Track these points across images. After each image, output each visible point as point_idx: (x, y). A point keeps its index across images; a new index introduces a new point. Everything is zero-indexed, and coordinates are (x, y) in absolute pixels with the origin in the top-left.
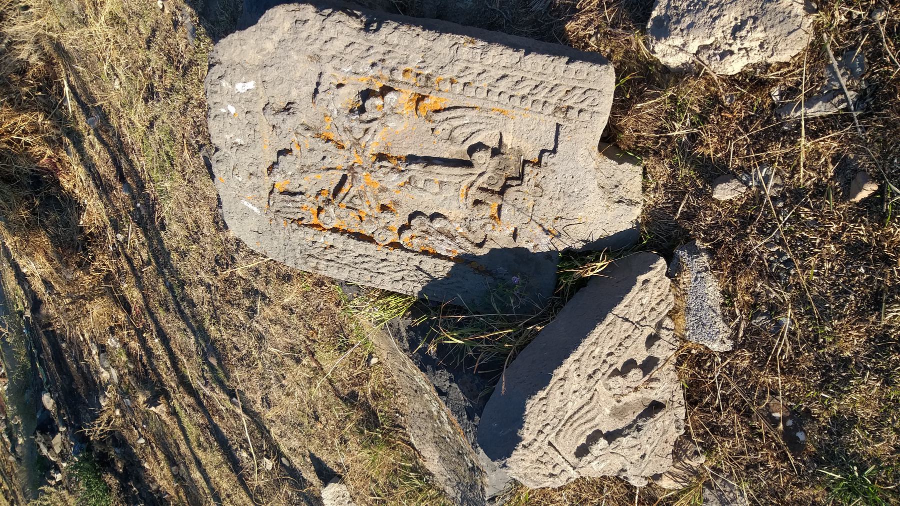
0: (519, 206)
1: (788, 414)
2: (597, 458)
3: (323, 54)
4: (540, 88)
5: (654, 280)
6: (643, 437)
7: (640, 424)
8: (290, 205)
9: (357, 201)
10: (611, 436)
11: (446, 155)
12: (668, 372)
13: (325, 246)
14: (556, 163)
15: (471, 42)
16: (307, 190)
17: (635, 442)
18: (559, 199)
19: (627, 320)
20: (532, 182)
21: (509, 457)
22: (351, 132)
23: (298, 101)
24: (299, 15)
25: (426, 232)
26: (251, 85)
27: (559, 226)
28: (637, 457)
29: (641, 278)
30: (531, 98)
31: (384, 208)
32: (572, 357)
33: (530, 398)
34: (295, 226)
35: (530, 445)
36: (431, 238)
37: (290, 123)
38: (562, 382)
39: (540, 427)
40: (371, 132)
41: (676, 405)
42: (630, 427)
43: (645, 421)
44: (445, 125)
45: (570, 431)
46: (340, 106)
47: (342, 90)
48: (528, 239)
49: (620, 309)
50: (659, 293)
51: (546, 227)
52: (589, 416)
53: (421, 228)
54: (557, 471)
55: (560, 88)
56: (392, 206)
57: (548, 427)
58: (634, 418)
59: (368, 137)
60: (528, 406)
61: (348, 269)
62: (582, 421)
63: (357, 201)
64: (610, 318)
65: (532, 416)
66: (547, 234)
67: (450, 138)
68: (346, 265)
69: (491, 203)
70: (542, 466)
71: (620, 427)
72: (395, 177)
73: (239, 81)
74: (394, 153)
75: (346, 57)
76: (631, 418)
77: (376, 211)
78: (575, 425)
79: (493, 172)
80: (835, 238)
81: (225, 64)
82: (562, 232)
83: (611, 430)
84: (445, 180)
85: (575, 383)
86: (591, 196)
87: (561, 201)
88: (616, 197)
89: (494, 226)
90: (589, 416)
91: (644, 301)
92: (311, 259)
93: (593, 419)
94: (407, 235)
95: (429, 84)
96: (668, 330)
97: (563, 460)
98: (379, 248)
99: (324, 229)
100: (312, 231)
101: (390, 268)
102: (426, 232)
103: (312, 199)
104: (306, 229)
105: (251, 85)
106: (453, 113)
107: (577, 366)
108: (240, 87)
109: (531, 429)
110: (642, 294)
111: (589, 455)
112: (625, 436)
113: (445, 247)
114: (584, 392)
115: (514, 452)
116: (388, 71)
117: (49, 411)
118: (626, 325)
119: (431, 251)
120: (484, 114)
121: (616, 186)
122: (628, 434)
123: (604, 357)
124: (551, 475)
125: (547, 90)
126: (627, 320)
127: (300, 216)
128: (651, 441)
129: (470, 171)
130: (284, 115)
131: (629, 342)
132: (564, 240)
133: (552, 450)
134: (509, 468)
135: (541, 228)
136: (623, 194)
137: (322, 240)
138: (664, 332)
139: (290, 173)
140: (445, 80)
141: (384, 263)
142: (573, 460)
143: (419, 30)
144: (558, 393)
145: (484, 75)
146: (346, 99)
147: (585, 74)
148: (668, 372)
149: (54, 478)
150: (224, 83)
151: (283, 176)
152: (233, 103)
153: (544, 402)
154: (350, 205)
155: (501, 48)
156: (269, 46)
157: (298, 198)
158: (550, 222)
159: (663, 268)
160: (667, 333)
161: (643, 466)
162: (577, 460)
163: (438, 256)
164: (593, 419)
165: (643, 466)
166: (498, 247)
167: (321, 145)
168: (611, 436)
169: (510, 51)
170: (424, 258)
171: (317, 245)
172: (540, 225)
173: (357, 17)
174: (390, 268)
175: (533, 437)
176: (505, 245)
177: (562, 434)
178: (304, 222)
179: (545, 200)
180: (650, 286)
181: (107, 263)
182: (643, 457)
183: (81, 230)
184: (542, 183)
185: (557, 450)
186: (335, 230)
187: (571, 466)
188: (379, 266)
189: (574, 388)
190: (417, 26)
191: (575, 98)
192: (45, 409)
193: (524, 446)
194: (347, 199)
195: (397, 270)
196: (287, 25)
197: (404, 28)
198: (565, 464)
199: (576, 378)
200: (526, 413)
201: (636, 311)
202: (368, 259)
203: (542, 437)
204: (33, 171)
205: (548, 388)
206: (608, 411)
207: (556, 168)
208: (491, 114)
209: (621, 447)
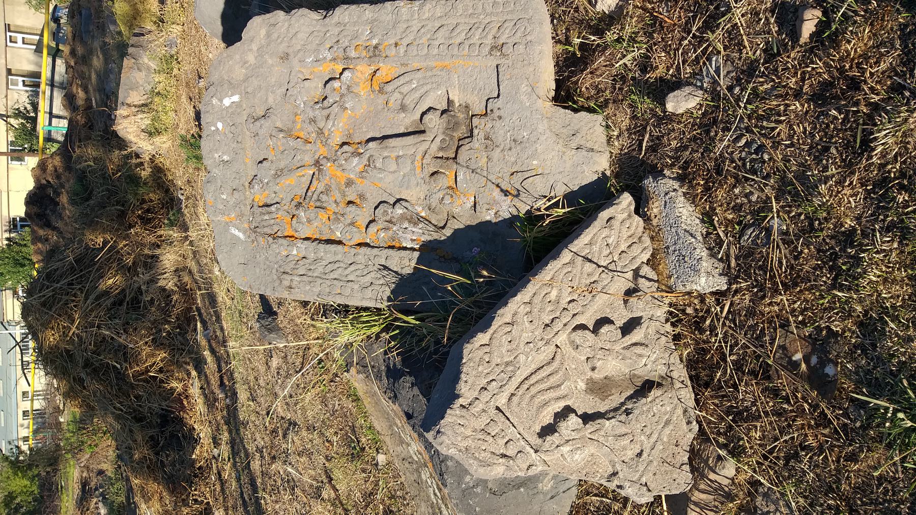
0: (473, 166)
1: (810, 348)
2: (568, 441)
3: (290, 51)
4: (473, 30)
5: (621, 217)
7: (630, 407)
8: (266, 217)
9: (324, 198)
10: (587, 418)
11: (402, 130)
12: (658, 336)
13: (298, 258)
14: (501, 107)
16: (282, 199)
17: (623, 429)
18: (510, 149)
19: (590, 261)
20: (482, 135)
21: (443, 418)
22: (315, 122)
23: (273, 106)
24: (272, 21)
25: (390, 222)
26: (236, 98)
27: (516, 180)
28: (630, 454)
29: (604, 215)
30: (467, 43)
31: (350, 202)
33: (468, 342)
34: (270, 239)
35: (470, 404)
36: (394, 229)
37: (266, 124)
40: (331, 117)
41: (678, 385)
42: (616, 410)
43: (635, 402)
44: (397, 95)
46: (305, 99)
48: (488, 207)
50: (629, 234)
51: (504, 188)
52: (553, 380)
53: (384, 218)
55: (492, 25)
56: (358, 201)
57: (494, 383)
58: (622, 400)
59: (330, 123)
60: (465, 352)
61: (319, 281)
63: (324, 198)
64: (566, 256)
65: (472, 364)
66: (506, 195)
67: (403, 108)
68: (317, 277)
69: (447, 173)
70: (491, 440)
71: (602, 410)
72: (356, 160)
73: (226, 96)
75: (308, 47)
76: (616, 399)
77: (342, 207)
78: (534, 390)
79: (444, 133)
80: (798, 95)
81: (216, 83)
82: (520, 188)
84: (401, 153)
85: (526, 331)
86: (543, 138)
87: (514, 150)
88: (574, 145)
89: (452, 196)
90: (553, 380)
91: (610, 241)
92: (285, 276)
93: (559, 386)
94: (373, 228)
95: (377, 53)
96: (650, 280)
97: (519, 436)
98: (346, 249)
101: (358, 273)
102: (390, 222)
103: (286, 207)
104: (281, 241)
105: (236, 98)
106: (402, 80)
107: (528, 309)
108: (227, 102)
109: (470, 382)
110: (606, 232)
111: (556, 434)
112: (608, 419)
113: (409, 236)
114: (540, 344)
115: (449, 411)
116: (342, 49)
118: (589, 267)
119: (397, 245)
120: (429, 74)
122: (613, 417)
124: (504, 456)
125: (480, 30)
126: (590, 261)
127: (276, 228)
128: (648, 431)
129: (421, 137)
132: (524, 199)
134: (443, 433)
135: (498, 189)
138: (643, 284)
139: (266, 181)
140: (390, 45)
141: (352, 268)
145: (423, 30)
146: (312, 93)
147: (512, 4)
148: (658, 336)
150: (215, 101)
151: (261, 185)
152: (221, 119)
153: (487, 349)
154: (318, 204)
156: (251, 58)
157: (273, 208)
158: (507, 179)
159: (630, 204)
160: (648, 284)
161: (641, 468)
162: (539, 441)
163: (405, 249)
165: (641, 468)
166: (462, 226)
167: (292, 143)
168: (587, 418)
170: (390, 252)
171: (291, 258)
172: (498, 186)
174: (358, 273)
175: (476, 394)
176: (469, 223)
177: (515, 399)
178: (279, 234)
179: (496, 154)
180: (616, 223)
181: (208, 495)
182: (640, 455)
183: (194, 462)
184: (491, 134)
185: (508, 419)
186: (307, 239)
188: (347, 272)
189: (526, 337)
191: (507, 31)
193: (462, 406)
194: (315, 197)
195: (365, 273)
196: (263, 32)
198: (523, 443)
200: (464, 361)
201: (600, 252)
202: (337, 265)
204: (163, 409)
205: (490, 331)
206: (582, 385)
207: (501, 113)
208: (435, 72)
209: (602, 433)
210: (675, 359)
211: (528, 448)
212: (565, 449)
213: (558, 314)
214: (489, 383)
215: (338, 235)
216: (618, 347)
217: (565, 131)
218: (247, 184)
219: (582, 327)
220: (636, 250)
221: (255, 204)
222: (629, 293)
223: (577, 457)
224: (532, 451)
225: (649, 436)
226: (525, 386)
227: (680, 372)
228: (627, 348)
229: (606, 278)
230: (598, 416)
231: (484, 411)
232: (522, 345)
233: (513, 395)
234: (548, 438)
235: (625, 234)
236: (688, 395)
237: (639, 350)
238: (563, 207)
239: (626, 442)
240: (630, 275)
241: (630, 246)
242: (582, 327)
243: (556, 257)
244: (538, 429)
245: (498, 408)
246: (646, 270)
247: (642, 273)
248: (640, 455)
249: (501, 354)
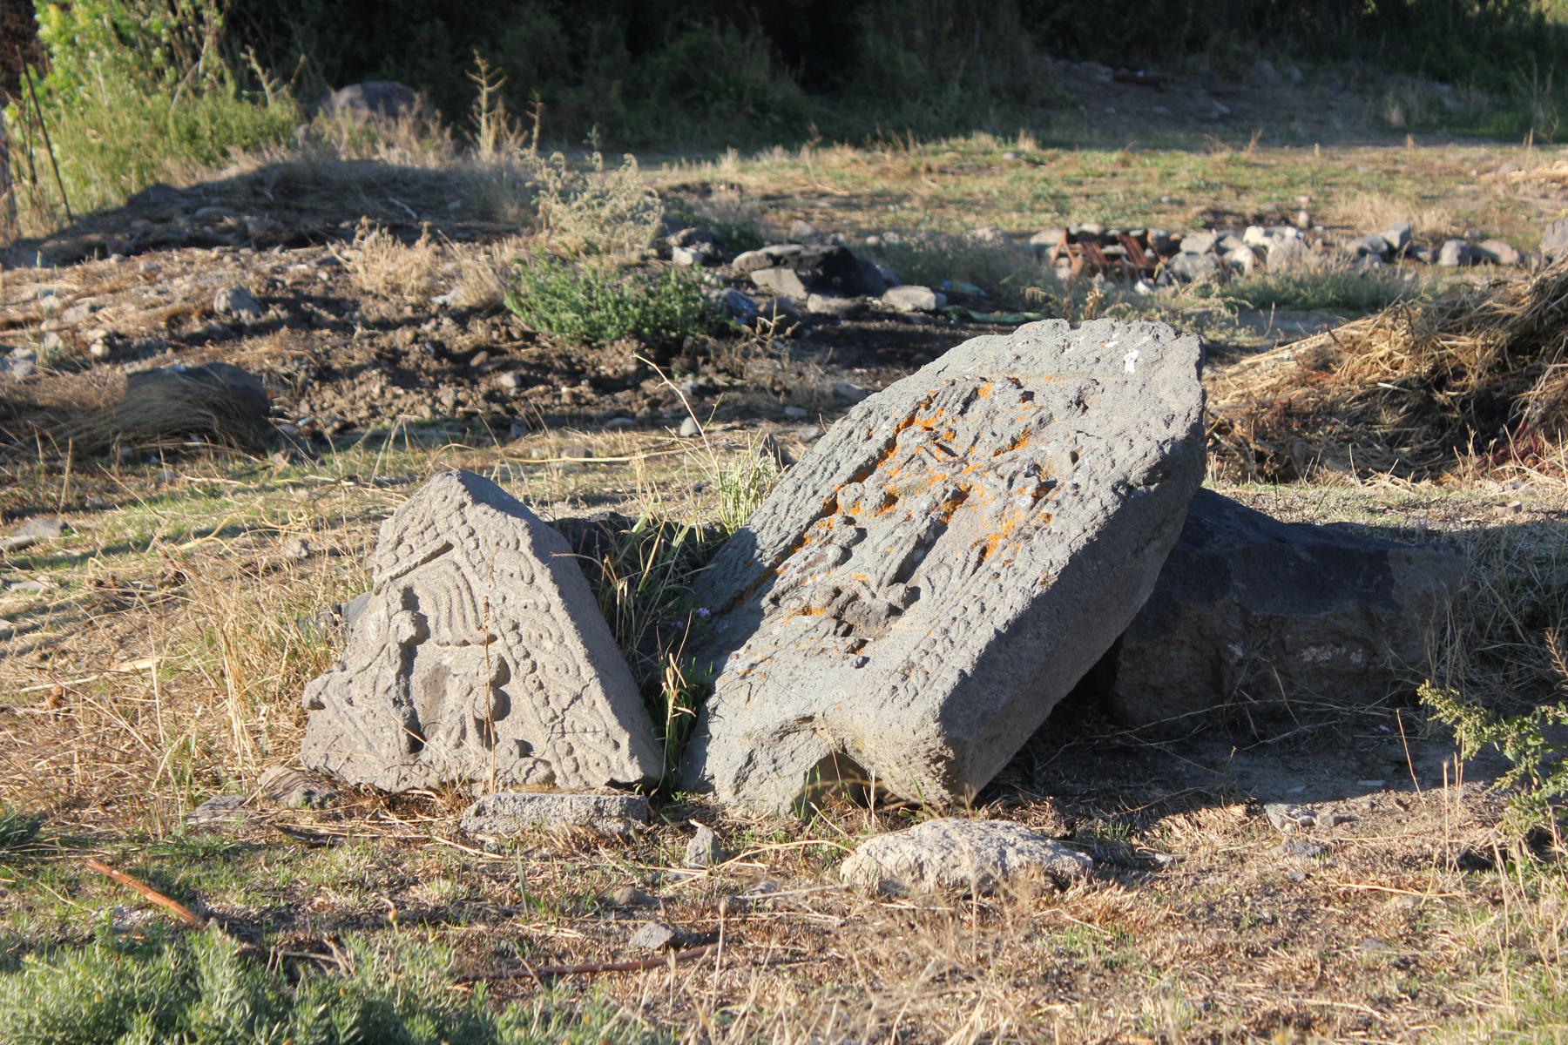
2: (390, 618)
5: (613, 757)
6: (383, 704)
9: (915, 465)
10: (408, 652)
15: (1043, 583)
17: (381, 688)
24: (1179, 421)
26: (1130, 368)
28: (356, 693)
29: (624, 740)
32: (556, 600)
37: (1058, 404)
38: (527, 579)
39: (479, 534)
41: (405, 771)
42: (407, 692)
45: (450, 585)
47: (1067, 459)
49: (596, 691)
52: (457, 619)
54: (403, 549)
60: (517, 520)
62: (455, 606)
64: (588, 672)
71: (413, 677)
74: (960, 512)
78: (454, 593)
83: (416, 661)
85: (518, 596)
90: (457, 619)
93: (450, 626)
99: (898, 431)
100: (903, 418)
103: (950, 423)
105: (1130, 368)
115: (462, 487)
117: (879, 294)
121: (775, 761)
123: (536, 655)
124: (400, 541)
128: (369, 718)
130: (1073, 395)
131: (539, 696)
133: (437, 545)
136: (759, 770)
137: (884, 427)
142: (404, 582)
143: (1091, 533)
144: (516, 570)
146: (1056, 466)
149: (685, 244)
153: (512, 545)
155: (1020, 608)
157: (959, 407)
159: (625, 775)
160: (525, 769)
164: (450, 626)
165: (336, 698)
168: (408, 652)
169: (1010, 616)
173: (1147, 482)
175: (470, 523)
177: (451, 569)
179: (798, 659)
180: (608, 748)
182: (350, 702)
185: (435, 555)
186: (891, 444)
187: (397, 576)
190: (1098, 534)
192: (890, 284)
193: (463, 505)
197: (1101, 518)
198: (405, 565)
199: (524, 602)
201: (579, 718)
203: (464, 531)
205: (529, 554)
206: (447, 661)
210: (433, 781)
211: (398, 570)
212: (383, 613)
213: (524, 643)
214: (477, 541)
215: (870, 482)
216: (467, 711)
217: (787, 751)
218: (1016, 376)
219: (503, 675)
220: (568, 764)
221: (983, 384)
222: (525, 749)
223: (371, 627)
224: (393, 573)
225: (363, 718)
226: (461, 585)
227: (418, 781)
228: (462, 719)
229: (546, 714)
230: (406, 669)
231: (450, 528)
232: (502, 589)
233: (458, 568)
234: (399, 596)
235: (592, 758)
236: (388, 783)
237: (455, 734)
238: (676, 711)
239: (368, 690)
240: (547, 757)
241: (575, 760)
242: (503, 675)
243: (592, 658)
244: (417, 592)
245: (448, 547)
246: (542, 771)
247: (540, 766)
248: (350, 702)
249: (506, 562)
